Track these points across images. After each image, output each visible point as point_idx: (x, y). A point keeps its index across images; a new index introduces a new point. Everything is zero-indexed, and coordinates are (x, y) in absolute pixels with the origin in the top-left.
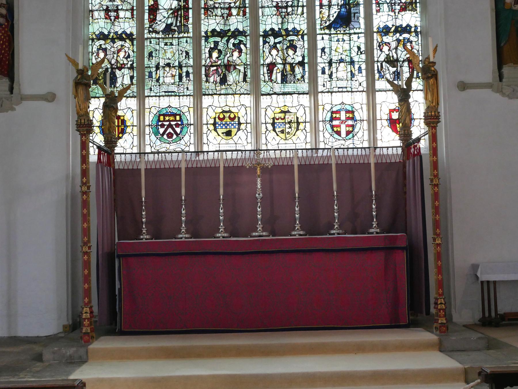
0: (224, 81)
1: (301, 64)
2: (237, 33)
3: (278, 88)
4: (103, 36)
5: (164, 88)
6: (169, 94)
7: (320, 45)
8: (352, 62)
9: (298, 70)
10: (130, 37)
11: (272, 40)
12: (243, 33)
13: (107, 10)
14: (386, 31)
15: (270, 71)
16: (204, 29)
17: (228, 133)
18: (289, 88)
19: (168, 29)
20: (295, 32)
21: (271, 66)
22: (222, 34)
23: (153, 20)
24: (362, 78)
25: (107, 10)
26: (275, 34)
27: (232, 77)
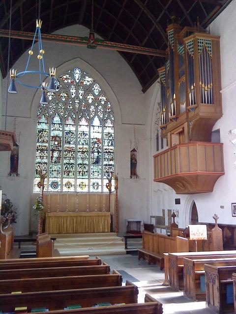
0: (68, 175)
1: (87, 172)
2: (72, 164)
3: (81, 177)
4: (39, 163)
5: (54, 176)
6: (55, 177)
7: (91, 167)
8: (98, 172)
9: (86, 173)
10: (46, 163)
11: (80, 166)
12: (73, 164)
13: (41, 157)
14: (106, 165)
15: (79, 173)
16: (64, 162)
17: (69, 187)
18: (84, 177)
19: (55, 162)
20: (86, 164)
21: (80, 172)
22: (68, 164)
23: (52, 159)
24: (100, 176)
25: (41, 157)
26: (81, 164)
27: (70, 174)
